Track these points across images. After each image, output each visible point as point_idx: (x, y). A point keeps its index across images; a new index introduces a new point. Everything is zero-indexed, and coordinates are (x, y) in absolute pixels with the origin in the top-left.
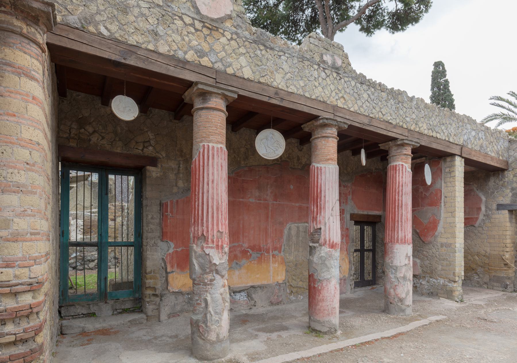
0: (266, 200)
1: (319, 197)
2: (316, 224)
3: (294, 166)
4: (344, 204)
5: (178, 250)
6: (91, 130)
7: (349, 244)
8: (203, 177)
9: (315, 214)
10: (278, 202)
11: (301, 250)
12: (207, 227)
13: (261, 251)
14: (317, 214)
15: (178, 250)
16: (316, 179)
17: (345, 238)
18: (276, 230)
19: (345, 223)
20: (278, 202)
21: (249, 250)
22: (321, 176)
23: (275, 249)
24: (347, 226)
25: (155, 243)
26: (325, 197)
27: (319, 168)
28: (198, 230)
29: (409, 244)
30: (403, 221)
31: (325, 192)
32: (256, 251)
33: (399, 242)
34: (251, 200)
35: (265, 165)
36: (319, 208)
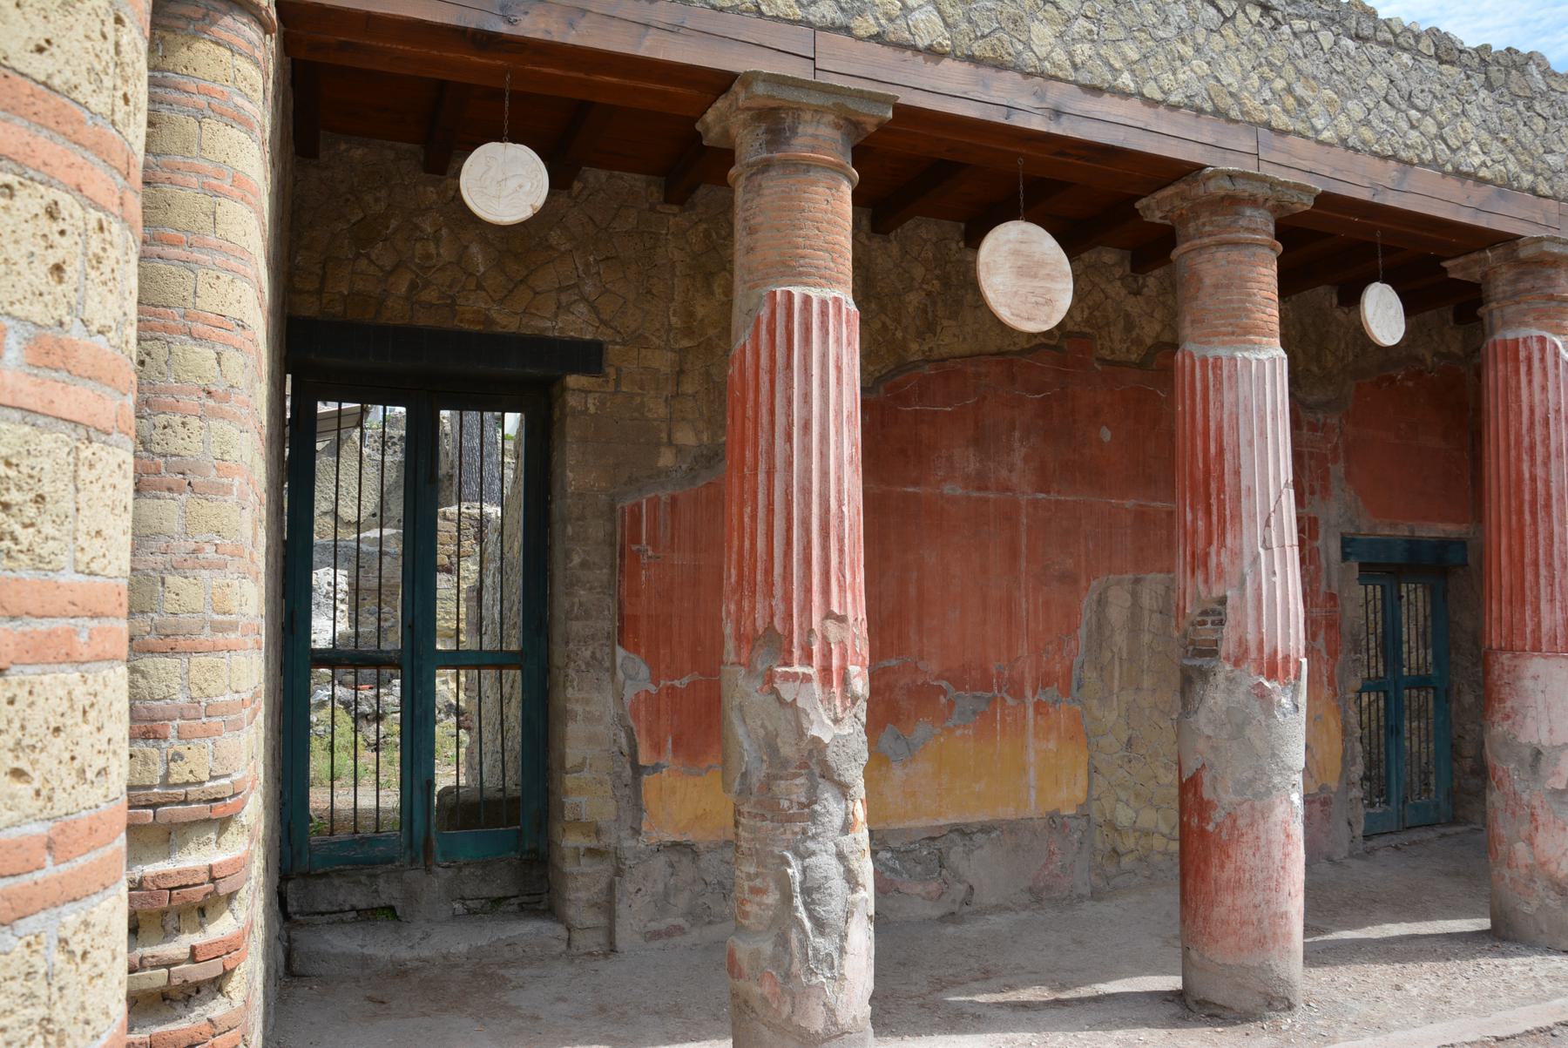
0: (1008, 489)
1: (1214, 474)
2: (1206, 581)
3: (1113, 352)
4: (1317, 497)
5: (677, 683)
6: (387, 261)
7: (1340, 657)
8: (772, 412)
9: (1201, 544)
10: (1053, 497)
11: (1147, 682)
12: (788, 599)
13: (989, 688)
14: (1210, 543)
15: (677, 683)
16: (1199, 407)
19: (1323, 575)
20: (1053, 497)
21: (944, 684)
22: (1219, 390)
23: (1045, 680)
24: (1329, 586)
25: (593, 656)
26: (1237, 473)
27: (1211, 360)
28: (753, 609)
30: (1557, 563)
31: (1237, 456)
32: (973, 688)
33: (1544, 648)
34: (948, 489)
35: (1000, 353)
36: (1215, 518)
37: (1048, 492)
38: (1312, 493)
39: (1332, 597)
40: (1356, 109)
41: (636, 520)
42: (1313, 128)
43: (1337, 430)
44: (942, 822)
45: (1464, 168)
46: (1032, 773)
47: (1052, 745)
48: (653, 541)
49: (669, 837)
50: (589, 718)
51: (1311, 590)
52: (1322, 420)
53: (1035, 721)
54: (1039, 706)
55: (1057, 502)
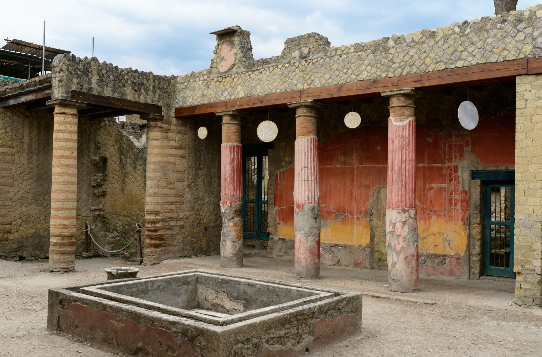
0: (352, 165)
4: (458, 159)
10: (363, 166)
17: (460, 204)
18: (361, 193)
20: (363, 166)
23: (360, 212)
24: (464, 188)
29: (393, 209)
34: (337, 166)
37: (362, 165)
38: (456, 158)
39: (465, 192)
40: (327, 76)
41: (277, 176)
42: (315, 85)
43: (469, 136)
44: (333, 243)
45: (360, 80)
46: (355, 234)
47: (361, 228)
48: (280, 180)
49: (281, 237)
50: (271, 213)
51: (455, 189)
52: (462, 133)
53: (357, 222)
54: (358, 218)
55: (365, 167)
